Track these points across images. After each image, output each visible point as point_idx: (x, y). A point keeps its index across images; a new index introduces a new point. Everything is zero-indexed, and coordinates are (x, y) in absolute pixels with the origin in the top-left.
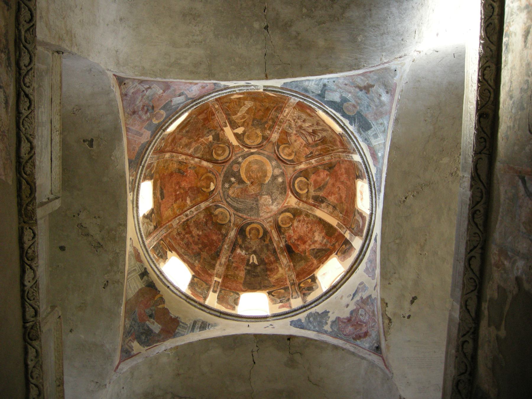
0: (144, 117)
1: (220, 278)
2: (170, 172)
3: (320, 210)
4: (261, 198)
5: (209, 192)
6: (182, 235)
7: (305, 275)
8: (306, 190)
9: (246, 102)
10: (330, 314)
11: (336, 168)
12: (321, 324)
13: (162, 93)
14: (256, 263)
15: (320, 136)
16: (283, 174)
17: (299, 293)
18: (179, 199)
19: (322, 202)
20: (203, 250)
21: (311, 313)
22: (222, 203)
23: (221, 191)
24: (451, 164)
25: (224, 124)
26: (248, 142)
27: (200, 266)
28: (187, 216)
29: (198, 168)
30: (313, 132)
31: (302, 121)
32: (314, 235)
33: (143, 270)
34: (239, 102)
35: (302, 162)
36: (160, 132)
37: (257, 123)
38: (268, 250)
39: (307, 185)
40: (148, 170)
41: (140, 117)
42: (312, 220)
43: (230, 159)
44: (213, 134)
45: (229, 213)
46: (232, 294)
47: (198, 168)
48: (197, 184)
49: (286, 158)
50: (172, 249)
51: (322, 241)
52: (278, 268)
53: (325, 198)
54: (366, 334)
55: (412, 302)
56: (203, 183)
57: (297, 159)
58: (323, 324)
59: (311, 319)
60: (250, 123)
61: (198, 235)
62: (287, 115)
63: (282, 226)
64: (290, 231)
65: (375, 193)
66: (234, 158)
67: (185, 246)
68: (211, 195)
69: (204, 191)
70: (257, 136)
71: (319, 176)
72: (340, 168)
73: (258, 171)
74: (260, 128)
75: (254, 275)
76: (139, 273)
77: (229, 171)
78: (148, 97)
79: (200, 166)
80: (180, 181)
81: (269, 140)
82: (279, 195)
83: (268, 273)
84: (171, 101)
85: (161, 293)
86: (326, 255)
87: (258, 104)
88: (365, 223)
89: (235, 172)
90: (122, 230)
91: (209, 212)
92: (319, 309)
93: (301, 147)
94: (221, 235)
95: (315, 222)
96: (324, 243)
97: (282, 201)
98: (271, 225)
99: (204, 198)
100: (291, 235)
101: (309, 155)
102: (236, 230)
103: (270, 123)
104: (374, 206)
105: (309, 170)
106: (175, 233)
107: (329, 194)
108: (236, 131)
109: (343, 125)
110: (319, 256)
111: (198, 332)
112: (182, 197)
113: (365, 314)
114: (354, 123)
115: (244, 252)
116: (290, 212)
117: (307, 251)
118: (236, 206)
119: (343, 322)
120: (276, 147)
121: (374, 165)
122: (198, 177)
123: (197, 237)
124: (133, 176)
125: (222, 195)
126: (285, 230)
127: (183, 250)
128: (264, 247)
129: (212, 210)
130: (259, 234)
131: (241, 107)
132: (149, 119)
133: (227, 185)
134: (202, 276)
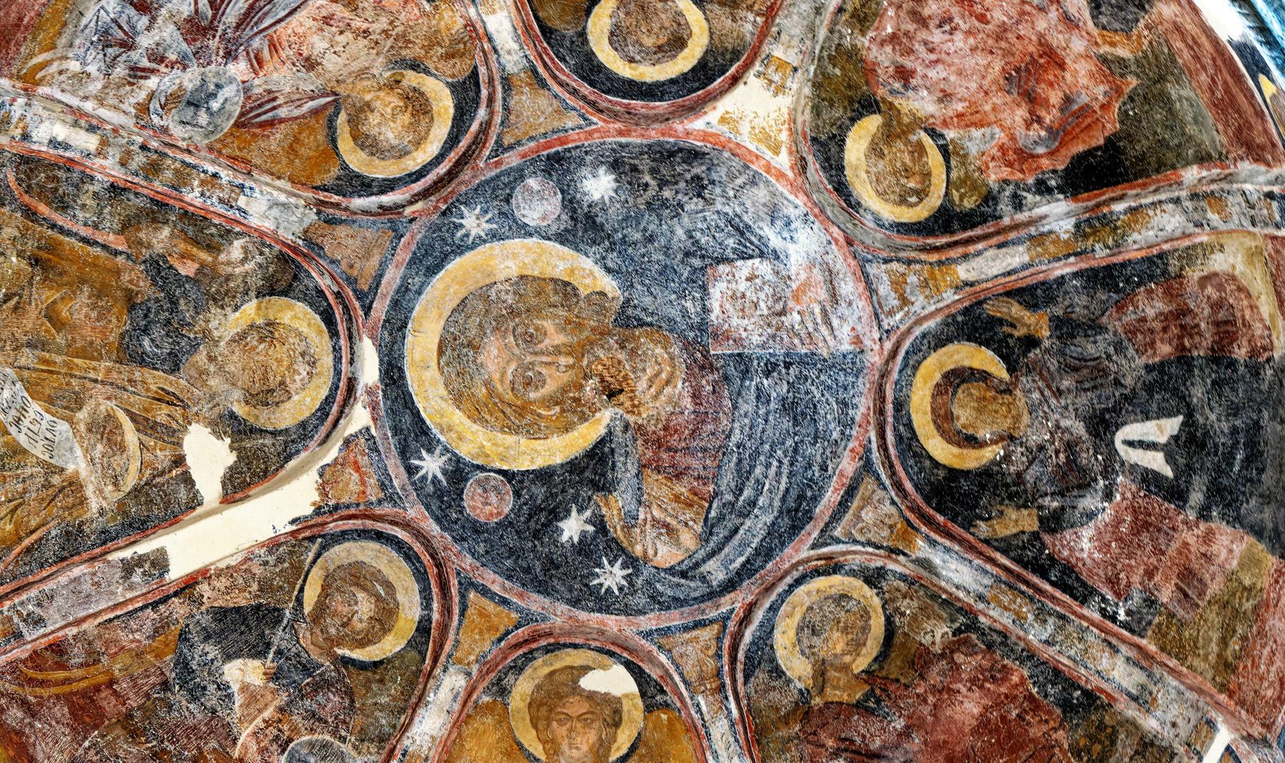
5: (649, 709)
14: (1170, 426)
16: (556, 159)
22: (732, 626)
23: (649, 622)
25: (136, 578)
31: (144, 20)
35: (469, 25)
37: (158, 332)
38: (1094, 327)
43: (419, 534)
44: (212, 651)
45: (817, 572)
49: (440, 131)
57: (449, 56)
60: (156, 379)
63: (935, 200)
64: (973, 149)
68: (671, 698)
69: (633, 748)
70: (268, 331)
73: (530, 339)
75: (1248, 461)
77: (512, 552)
81: (295, 249)
82: (709, 202)
89: (517, 511)
91: (786, 721)
93: (358, 23)
94: (959, 658)
97: (753, 182)
98: (925, 284)
99: (686, 745)
102: (933, 543)
103: (161, 238)
108: (209, 485)
115: (1089, 502)
117: (1105, 49)
118: (768, 519)
120: (358, 202)
125: (674, 618)
126: (963, 182)
128: (1073, 350)
130: (984, 376)
133: (612, 576)
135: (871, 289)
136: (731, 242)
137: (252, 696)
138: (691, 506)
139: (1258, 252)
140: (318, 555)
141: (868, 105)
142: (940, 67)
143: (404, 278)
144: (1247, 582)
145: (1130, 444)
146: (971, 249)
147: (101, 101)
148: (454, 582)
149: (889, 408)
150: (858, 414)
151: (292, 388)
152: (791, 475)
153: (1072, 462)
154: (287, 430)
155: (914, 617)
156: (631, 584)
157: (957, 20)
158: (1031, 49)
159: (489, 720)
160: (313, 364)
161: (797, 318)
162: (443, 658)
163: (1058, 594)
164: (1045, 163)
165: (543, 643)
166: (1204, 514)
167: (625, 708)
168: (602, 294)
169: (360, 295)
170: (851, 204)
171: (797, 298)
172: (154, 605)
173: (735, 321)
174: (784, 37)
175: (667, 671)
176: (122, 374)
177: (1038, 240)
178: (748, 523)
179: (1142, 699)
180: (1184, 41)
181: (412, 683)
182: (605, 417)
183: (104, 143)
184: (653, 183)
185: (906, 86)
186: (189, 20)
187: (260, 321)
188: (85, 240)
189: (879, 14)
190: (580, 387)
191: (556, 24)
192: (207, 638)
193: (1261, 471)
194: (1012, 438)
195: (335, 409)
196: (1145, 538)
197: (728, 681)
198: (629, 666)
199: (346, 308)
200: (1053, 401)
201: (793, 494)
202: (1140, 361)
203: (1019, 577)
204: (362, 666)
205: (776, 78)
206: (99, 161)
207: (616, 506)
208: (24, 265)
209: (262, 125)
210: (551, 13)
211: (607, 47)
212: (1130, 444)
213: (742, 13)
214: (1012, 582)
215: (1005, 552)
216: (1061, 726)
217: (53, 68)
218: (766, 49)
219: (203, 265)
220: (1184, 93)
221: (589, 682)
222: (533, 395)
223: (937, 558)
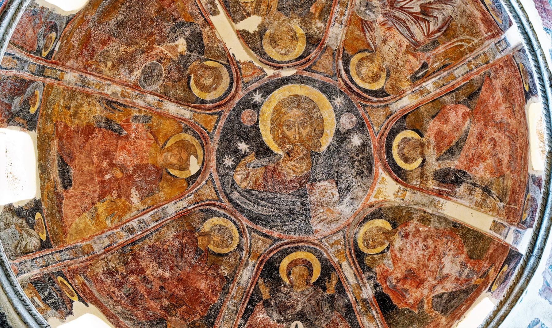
3: (454, 202)
5: (187, 179)
8: (420, 160)
11: (484, 94)
15: (440, 17)
16: (363, 125)
18: (110, 192)
19: (458, 182)
20: (173, 313)
22: (218, 203)
23: (215, 176)
25: (209, 6)
28: (130, 231)
29: (155, 118)
32: (441, 263)
35: (404, 92)
42: (436, 228)
43: (234, 96)
44: (188, 34)
45: (239, 229)
47: (155, 118)
49: (367, 86)
51: (461, 273)
57: (393, 86)
61: (161, 278)
63: (366, 251)
64: (385, 261)
68: (191, 186)
69: (173, 176)
70: (295, 39)
71: (447, 121)
72: (492, 90)
73: (303, 124)
77: (232, 128)
79: (159, 114)
80: (112, 148)
81: (323, 44)
82: (355, 177)
86: (468, 300)
91: (189, 225)
93: (400, 55)
94: (218, 279)
95: (443, 234)
96: (464, 277)
97: (364, 191)
99: (177, 193)
101: (418, 72)
102: (254, 266)
105: (423, 109)
106: (100, 269)
107: (471, 161)
108: (242, 25)
110: (451, 307)
112: (119, 188)
115: (275, 315)
117: (426, 301)
118: (254, 210)
120: (340, 62)
122: (157, 141)
123: (156, 284)
125: (218, 184)
127: (119, 308)
128: (324, 303)
129: (196, 220)
130: (311, 275)
133: (228, 161)
135: (334, 234)
136: (343, 186)
137: (174, 49)
138: (255, 184)
140: (223, 64)
141: (394, 225)
142: (411, 247)
143: (317, 81)
146: (352, 265)
148: (220, 110)
149: (296, 245)
150: (292, 235)
151: (277, 48)
152: (270, 216)
153: (287, 308)
154: (263, 49)
155: (229, 263)
156: (227, 168)
158: (422, 276)
159: (176, 127)
161: (321, 211)
162: (195, 109)
163: (244, 309)
164: (384, 286)
165: (204, 142)
167: (186, 172)
168: (321, 146)
169: (310, 67)
170: (361, 224)
171: (327, 210)
172: (201, 13)
173: (317, 191)
174: (413, 195)
175: (200, 184)
177: (359, 287)
178: (252, 204)
181: (185, 100)
182: (280, 152)
184: (359, 158)
185: (403, 237)
187: (298, 35)
189: (425, 225)
190: (289, 143)
191: (408, 120)
192: (192, 31)
194: (292, 287)
195: (272, 63)
197: (199, 204)
198: (200, 171)
199: (305, 63)
200: (306, 299)
201: (264, 217)
203: (247, 295)
204: (188, 83)
205: (400, 194)
207: (252, 160)
209: (363, 28)
210: (411, 118)
213: (419, 180)
215: (255, 289)
216: (201, 316)
218: (409, 189)
219: (314, 14)
221: (192, 158)
222: (284, 128)
223: (250, 267)
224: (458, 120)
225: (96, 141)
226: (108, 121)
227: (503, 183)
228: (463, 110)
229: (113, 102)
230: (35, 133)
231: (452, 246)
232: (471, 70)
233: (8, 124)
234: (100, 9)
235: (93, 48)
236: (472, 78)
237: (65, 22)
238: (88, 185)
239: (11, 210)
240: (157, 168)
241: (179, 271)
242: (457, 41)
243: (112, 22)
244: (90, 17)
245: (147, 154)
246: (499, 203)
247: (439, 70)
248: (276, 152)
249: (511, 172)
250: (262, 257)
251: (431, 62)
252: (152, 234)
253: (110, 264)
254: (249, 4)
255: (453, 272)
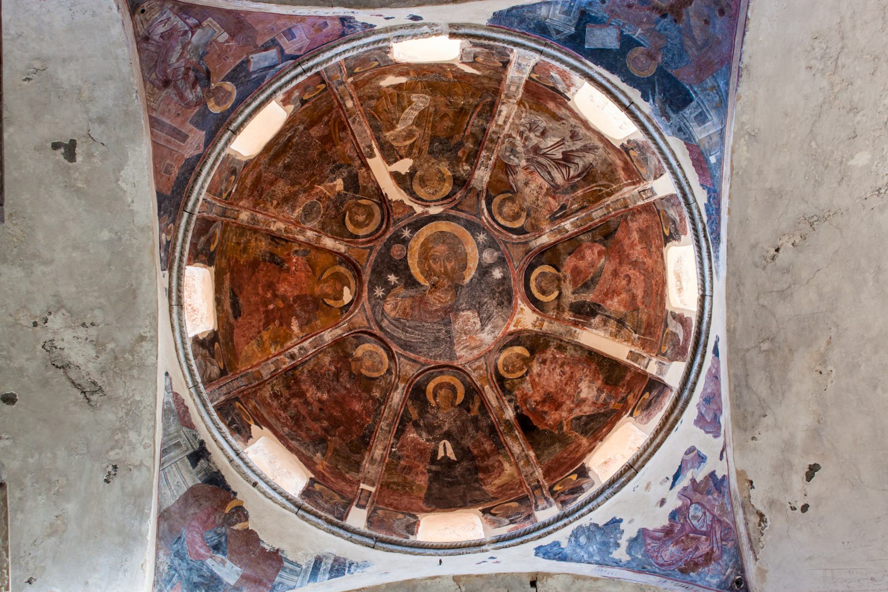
0: (190, 96)
1: (373, 485)
2: (252, 259)
3: (589, 331)
4: (456, 318)
5: (341, 309)
6: (283, 400)
7: (563, 468)
8: (556, 293)
9: (414, 97)
10: (622, 526)
11: (619, 234)
12: (606, 547)
13: (227, 41)
14: (453, 457)
15: (581, 164)
16: (504, 260)
17: (551, 499)
19: (593, 314)
20: (333, 433)
21: (581, 526)
23: (367, 306)
24: (874, 167)
25: (367, 149)
26: (421, 192)
27: (325, 463)
29: (313, 252)
30: (563, 159)
31: (538, 134)
32: (579, 388)
33: (197, 447)
34: (398, 95)
36: (226, 136)
37: (440, 147)
38: (477, 429)
39: (557, 282)
40: (203, 239)
41: (181, 96)
42: (572, 356)
43: (384, 232)
44: (345, 175)
46: (400, 516)
48: (313, 289)
49: (508, 224)
50: (261, 422)
51: (598, 398)
52: (501, 464)
53: (599, 306)
54: (708, 558)
55: (810, 475)
56: (327, 289)
57: (532, 224)
58: (609, 547)
59: (583, 540)
60: (426, 148)
61: (320, 401)
62: (505, 122)
63: (506, 375)
64: (524, 385)
65: (708, 248)
66: (392, 229)
67: (290, 423)
70: (442, 180)
71: (583, 258)
72: (629, 231)
73: (448, 258)
74: (448, 159)
75: (449, 482)
76: (188, 453)
78: (196, 48)
80: (275, 280)
82: (496, 308)
83: (481, 476)
84: (248, 61)
85: (238, 497)
86: (607, 423)
87: (441, 100)
88: (690, 331)
90: (146, 351)
91: (343, 351)
92: (600, 516)
93: (540, 197)
94: (371, 401)
95: (579, 361)
96: (601, 401)
97: (504, 320)
98: (480, 375)
100: (526, 394)
101: (557, 212)
102: (403, 389)
103: (469, 145)
104: (708, 279)
105: (560, 247)
106: (267, 392)
107: (606, 294)
109: (627, 104)
110: (591, 429)
111: (326, 581)
113: (705, 513)
114: (653, 96)
115: (424, 435)
116: (523, 345)
117: (565, 423)
118: (403, 337)
119: (654, 538)
120: (483, 202)
121: (702, 185)
122: (314, 273)
123: (315, 407)
124: (168, 233)
125: (369, 313)
126: (513, 383)
127: (286, 429)
128: (469, 424)
129: (350, 346)
130: (455, 397)
131: (403, 110)
132: (201, 102)
133: (379, 292)
134: (332, 482)
139: (514, 478)
141: (532, 351)
144: (414, 488)
145: (444, 445)
146: (494, 389)
147: (512, 124)
148: (371, 244)
151: (426, 189)
153: (434, 428)
154: (412, 188)
155: (380, 386)
157: (564, 377)
159: (331, 260)
160: (433, 194)
161: (465, 338)
163: (395, 429)
166: (429, 471)
168: (464, 279)
175: (353, 312)
176: (427, 137)
179: (372, 461)
180: (575, 448)
183: (500, 126)
185: (540, 363)
186: (539, 147)
187: (445, 177)
188: (468, 122)
190: (435, 276)
191: (545, 256)
192: (348, 172)
193: (447, 487)
194: (438, 408)
195: (420, 202)
196: (418, 454)
198: (352, 301)
199: (451, 202)
200: (452, 419)
201: (411, 344)
202: (470, 445)
205: (537, 324)
206: (494, 125)
208: (461, 106)
209: (506, 171)
210: (549, 254)
211: (540, 271)
212: (444, 445)
213: (556, 311)
214: (396, 414)
215: (404, 411)
216: (358, 436)
217: (523, 109)
218: (546, 319)
219: (461, 158)
220: (557, 449)
221: (346, 289)
222: (431, 261)
224: (594, 257)
225: (262, 273)
226: (272, 255)
227: (638, 316)
228: (599, 249)
229: (277, 237)
230: (213, 269)
231: (588, 373)
232: (609, 212)
233: (195, 262)
234: (271, 153)
235: (263, 188)
236: (609, 220)
237: (243, 166)
238: (254, 314)
239: (196, 341)
240: (314, 298)
241: (336, 394)
242: (596, 186)
243: (280, 165)
244: (262, 161)
245: (305, 285)
246: (634, 334)
247: (577, 211)
248: (423, 283)
249: (646, 306)
250: (410, 380)
251: (569, 204)
252: (310, 359)
253: (275, 388)
254: (402, 148)
255: (590, 396)
